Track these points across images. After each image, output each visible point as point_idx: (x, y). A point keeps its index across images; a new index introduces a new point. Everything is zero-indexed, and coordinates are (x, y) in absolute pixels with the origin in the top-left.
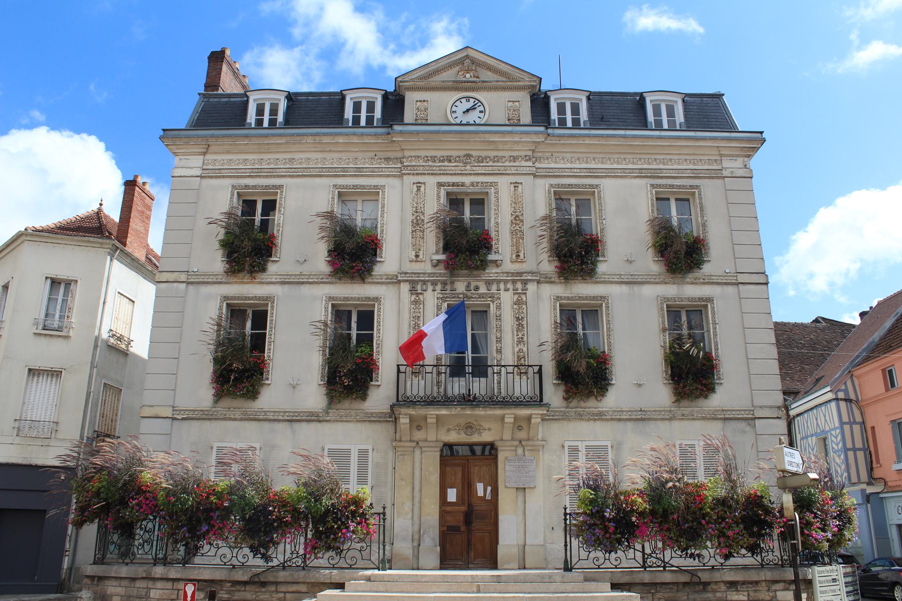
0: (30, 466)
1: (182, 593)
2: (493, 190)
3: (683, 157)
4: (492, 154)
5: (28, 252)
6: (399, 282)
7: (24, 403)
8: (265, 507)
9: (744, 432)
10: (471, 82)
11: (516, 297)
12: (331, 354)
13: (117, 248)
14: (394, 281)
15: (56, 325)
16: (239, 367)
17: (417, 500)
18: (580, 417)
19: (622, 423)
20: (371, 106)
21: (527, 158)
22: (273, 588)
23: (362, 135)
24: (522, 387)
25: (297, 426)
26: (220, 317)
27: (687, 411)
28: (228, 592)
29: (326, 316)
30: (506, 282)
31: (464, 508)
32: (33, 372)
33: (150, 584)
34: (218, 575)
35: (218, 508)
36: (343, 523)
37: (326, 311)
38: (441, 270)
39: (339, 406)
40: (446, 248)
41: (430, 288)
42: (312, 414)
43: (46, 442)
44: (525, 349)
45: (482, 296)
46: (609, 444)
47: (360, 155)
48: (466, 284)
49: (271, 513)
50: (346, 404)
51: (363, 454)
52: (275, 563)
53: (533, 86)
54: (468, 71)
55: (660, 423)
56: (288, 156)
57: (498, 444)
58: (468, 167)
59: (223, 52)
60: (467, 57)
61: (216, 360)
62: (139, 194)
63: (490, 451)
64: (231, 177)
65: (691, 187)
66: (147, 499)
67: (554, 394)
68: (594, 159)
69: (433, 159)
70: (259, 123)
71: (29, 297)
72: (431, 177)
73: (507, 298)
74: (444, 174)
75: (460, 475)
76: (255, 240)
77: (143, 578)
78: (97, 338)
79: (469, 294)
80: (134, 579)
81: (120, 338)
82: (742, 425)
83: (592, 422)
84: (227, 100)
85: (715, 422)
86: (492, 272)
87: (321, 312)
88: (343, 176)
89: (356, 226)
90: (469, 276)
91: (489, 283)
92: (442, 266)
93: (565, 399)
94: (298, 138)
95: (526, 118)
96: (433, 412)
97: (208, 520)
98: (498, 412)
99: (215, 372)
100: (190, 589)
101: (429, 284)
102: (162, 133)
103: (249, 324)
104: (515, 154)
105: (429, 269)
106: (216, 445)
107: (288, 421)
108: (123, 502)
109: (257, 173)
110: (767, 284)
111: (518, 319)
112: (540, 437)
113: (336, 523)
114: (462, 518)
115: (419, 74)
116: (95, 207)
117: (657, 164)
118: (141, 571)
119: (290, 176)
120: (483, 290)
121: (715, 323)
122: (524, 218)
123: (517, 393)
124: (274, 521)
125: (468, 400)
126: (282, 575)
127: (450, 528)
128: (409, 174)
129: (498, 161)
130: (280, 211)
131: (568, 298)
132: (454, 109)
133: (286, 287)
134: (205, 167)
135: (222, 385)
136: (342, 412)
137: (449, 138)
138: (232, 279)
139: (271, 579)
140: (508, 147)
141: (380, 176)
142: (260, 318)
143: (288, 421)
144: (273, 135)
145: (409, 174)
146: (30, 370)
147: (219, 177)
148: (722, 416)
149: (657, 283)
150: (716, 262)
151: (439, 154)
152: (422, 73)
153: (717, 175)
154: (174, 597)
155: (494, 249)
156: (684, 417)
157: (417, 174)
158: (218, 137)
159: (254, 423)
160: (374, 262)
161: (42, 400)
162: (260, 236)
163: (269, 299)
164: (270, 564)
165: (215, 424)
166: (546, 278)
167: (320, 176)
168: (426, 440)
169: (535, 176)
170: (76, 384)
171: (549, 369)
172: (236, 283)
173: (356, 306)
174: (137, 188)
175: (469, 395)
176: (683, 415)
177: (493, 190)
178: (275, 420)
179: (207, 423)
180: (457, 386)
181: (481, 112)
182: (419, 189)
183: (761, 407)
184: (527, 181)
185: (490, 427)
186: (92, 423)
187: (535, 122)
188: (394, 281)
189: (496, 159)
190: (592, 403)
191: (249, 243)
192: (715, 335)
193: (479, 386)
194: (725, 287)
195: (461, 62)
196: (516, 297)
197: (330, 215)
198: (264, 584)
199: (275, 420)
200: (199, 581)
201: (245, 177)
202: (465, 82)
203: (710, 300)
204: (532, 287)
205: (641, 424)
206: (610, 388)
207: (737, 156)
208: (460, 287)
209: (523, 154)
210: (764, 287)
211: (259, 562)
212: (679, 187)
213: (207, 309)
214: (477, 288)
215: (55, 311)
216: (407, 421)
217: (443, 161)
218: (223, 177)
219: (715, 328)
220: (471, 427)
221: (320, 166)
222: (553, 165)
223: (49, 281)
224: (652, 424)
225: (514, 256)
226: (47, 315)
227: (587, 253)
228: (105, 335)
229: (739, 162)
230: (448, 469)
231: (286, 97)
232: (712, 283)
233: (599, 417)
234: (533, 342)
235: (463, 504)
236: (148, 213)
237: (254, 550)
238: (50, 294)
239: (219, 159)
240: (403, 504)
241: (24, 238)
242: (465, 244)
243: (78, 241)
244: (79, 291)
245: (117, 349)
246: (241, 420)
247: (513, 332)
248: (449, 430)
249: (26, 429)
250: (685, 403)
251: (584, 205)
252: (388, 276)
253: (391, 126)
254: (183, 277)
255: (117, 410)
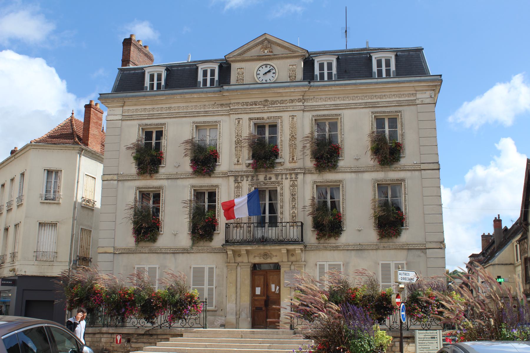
0: (44, 277)
1: (115, 339)
2: (280, 121)
3: (393, 93)
4: (280, 99)
5: (33, 155)
6: (229, 176)
7: (38, 242)
8: (149, 300)
9: (420, 256)
10: (267, 56)
11: (292, 182)
12: (193, 218)
13: (83, 149)
14: (226, 175)
15: (52, 196)
16: (147, 226)
17: (238, 294)
18: (326, 249)
19: (349, 251)
20: (213, 72)
21: (299, 100)
22: (155, 337)
23: (207, 92)
24: (294, 233)
25: (177, 255)
26: (136, 198)
27: (386, 245)
28: (136, 339)
29: (191, 196)
30: (286, 174)
31: (264, 298)
32: (42, 225)
33: (101, 336)
34: (131, 331)
35: (129, 300)
36: (185, 306)
37: (191, 193)
38: (250, 169)
39: (197, 245)
40: (253, 157)
41: (245, 179)
42: (184, 249)
43: (51, 263)
44: (296, 212)
45: (273, 183)
46: (341, 263)
47: (207, 103)
48: (264, 176)
49: (152, 302)
50: (201, 243)
51: (211, 270)
52: (156, 325)
53: (304, 55)
54: (266, 48)
55: (370, 251)
56: (168, 106)
57: (280, 264)
58: (266, 108)
59: (130, 39)
60: (266, 39)
61: (135, 223)
62: (94, 112)
63: (277, 267)
64: (137, 119)
65: (396, 112)
66: (98, 297)
67: (311, 236)
68: (339, 98)
69: (247, 104)
70: (152, 86)
71: (37, 182)
72: (246, 115)
73: (287, 183)
74: (252, 113)
75: (262, 280)
76: (152, 155)
77: (98, 333)
78: (75, 202)
79: (266, 182)
80: (94, 334)
81: (88, 201)
82: (419, 252)
83: (332, 251)
84: (133, 72)
85: (403, 251)
86: (278, 169)
87: (188, 195)
88: (198, 116)
89: (205, 145)
90: (266, 172)
91: (277, 175)
92: (251, 167)
93: (317, 239)
94: (172, 96)
95: (300, 75)
96: (243, 248)
97: (125, 306)
98: (278, 247)
99: (134, 228)
100: (119, 337)
101: (245, 177)
102: (99, 96)
103: (151, 202)
104: (292, 98)
105: (244, 168)
106: (136, 266)
107: (172, 253)
108: (88, 298)
109: (151, 117)
110: (439, 169)
111: (292, 194)
112: (303, 260)
113: (181, 306)
114: (263, 303)
115: (238, 52)
116: (69, 116)
117: (377, 99)
118: (97, 330)
119: (169, 118)
120: (273, 179)
121: (405, 194)
122: (297, 137)
123: (292, 236)
124: (154, 306)
125: (264, 241)
126: (159, 331)
127: (257, 308)
128: (233, 114)
129: (283, 103)
130: (165, 138)
131: (321, 182)
132: (258, 72)
133: (170, 181)
134: (124, 114)
135: (138, 236)
136: (200, 248)
137: (255, 92)
138: (141, 178)
139: (154, 333)
140: (288, 94)
141: (218, 115)
142: (157, 197)
143: (172, 253)
144: (159, 95)
145: (233, 114)
146: (40, 223)
147: (131, 120)
148: (407, 248)
149: (372, 171)
150: (409, 157)
151: (250, 101)
152: (240, 51)
153: (412, 103)
154: (112, 341)
155: (280, 156)
156: (384, 248)
157: (238, 113)
158: (128, 97)
159: (155, 255)
160: (214, 166)
161: (48, 240)
162: (154, 153)
163: (160, 187)
164: (154, 326)
165: (135, 255)
166: (309, 171)
167: (186, 117)
168: (243, 262)
169: (304, 111)
170: (65, 230)
171: (309, 221)
172: (143, 179)
173: (207, 190)
174: (92, 109)
175: (263, 239)
176: (384, 247)
177: (280, 121)
178: (166, 253)
179: (131, 255)
180: (259, 233)
181: (274, 73)
182: (239, 122)
183: (430, 242)
184: (299, 114)
185: (277, 254)
186: (76, 251)
187: (305, 79)
188: (226, 175)
189: (282, 102)
190: (332, 241)
191: (148, 157)
192: (405, 201)
193: (271, 233)
194: (413, 172)
195: (262, 42)
196: (292, 182)
197: (191, 142)
198: (151, 335)
199: (166, 253)
200: (123, 334)
201: (145, 119)
202: (264, 56)
203: (403, 180)
204: (300, 177)
205: (360, 252)
206: (342, 232)
207: (427, 90)
208: (261, 178)
209: (297, 98)
210: (437, 171)
211: (149, 325)
212: (389, 112)
213: (129, 194)
214: (270, 178)
215: (51, 188)
216: (231, 252)
217: (252, 105)
218: (134, 119)
219: (405, 197)
220: (266, 255)
221: (185, 111)
222: (315, 104)
223: (46, 172)
224: (366, 253)
225: (291, 159)
226: (46, 191)
227: (331, 156)
228: (79, 200)
229: (428, 94)
230: (256, 277)
231: (166, 70)
232: (405, 170)
233: (336, 248)
234: (300, 206)
235: (264, 295)
236: (100, 122)
237: (147, 319)
238: (47, 179)
239: (131, 109)
240: (231, 296)
241: (30, 147)
242: (264, 153)
243: (61, 147)
244: (63, 176)
245: (87, 207)
246: (149, 253)
247: (290, 202)
248: (255, 257)
249: (41, 256)
250: (385, 240)
251: (334, 126)
252: (223, 173)
253: (222, 86)
254: (115, 177)
255: (90, 242)
